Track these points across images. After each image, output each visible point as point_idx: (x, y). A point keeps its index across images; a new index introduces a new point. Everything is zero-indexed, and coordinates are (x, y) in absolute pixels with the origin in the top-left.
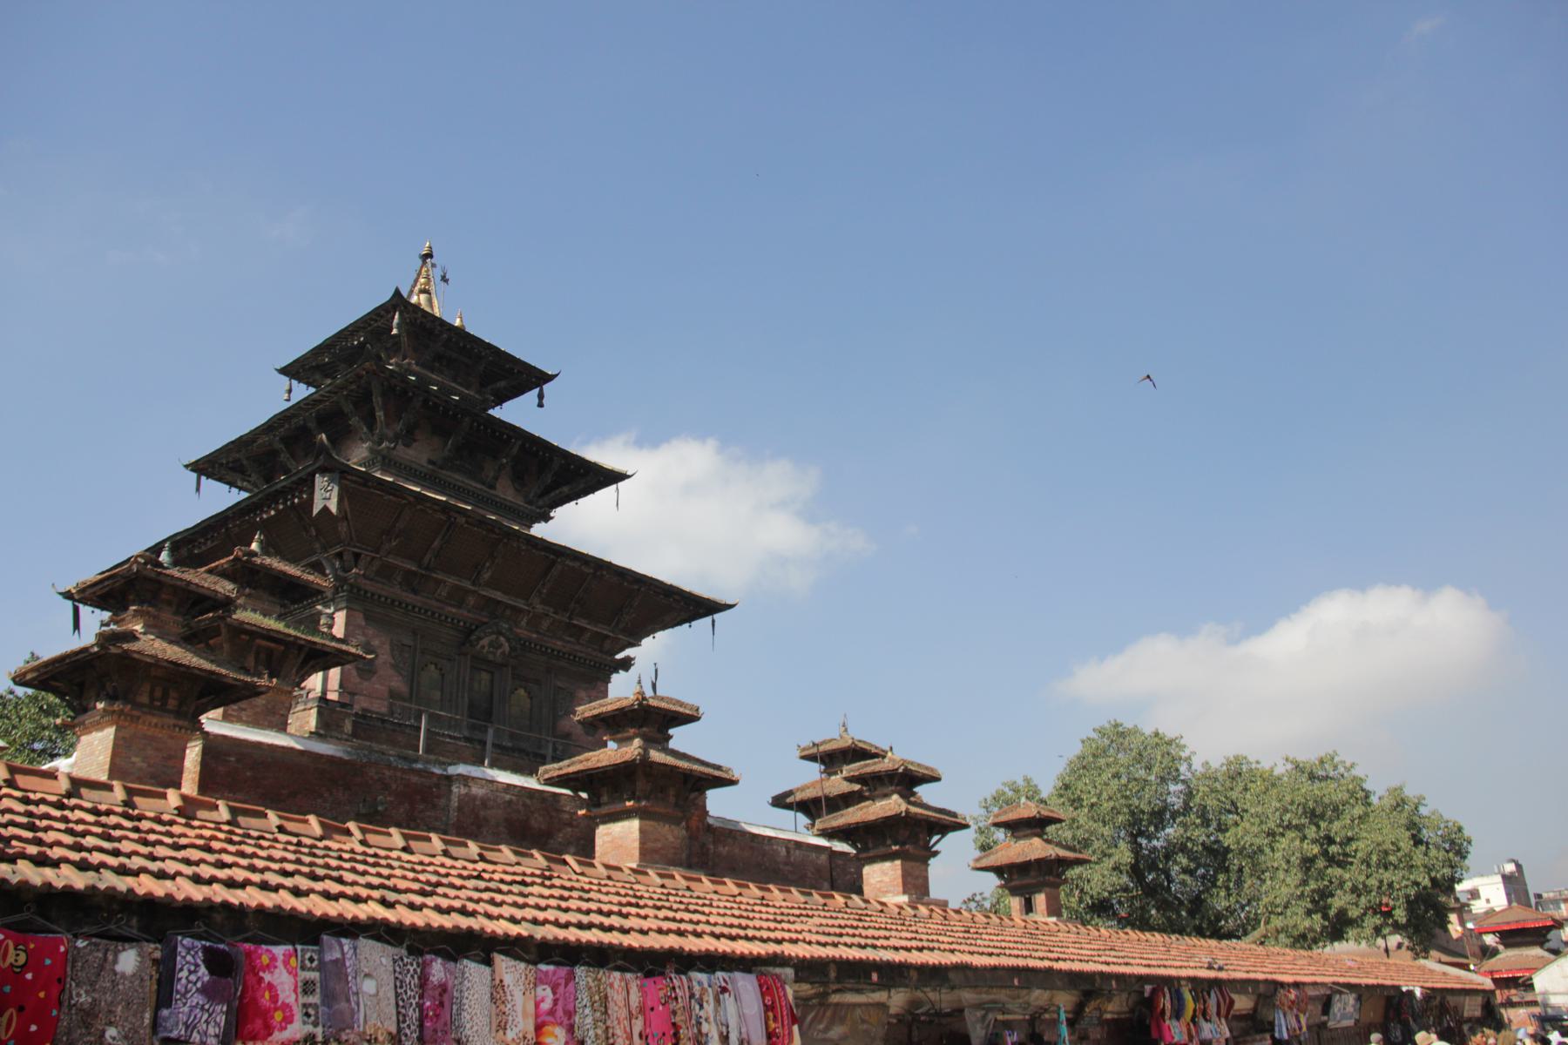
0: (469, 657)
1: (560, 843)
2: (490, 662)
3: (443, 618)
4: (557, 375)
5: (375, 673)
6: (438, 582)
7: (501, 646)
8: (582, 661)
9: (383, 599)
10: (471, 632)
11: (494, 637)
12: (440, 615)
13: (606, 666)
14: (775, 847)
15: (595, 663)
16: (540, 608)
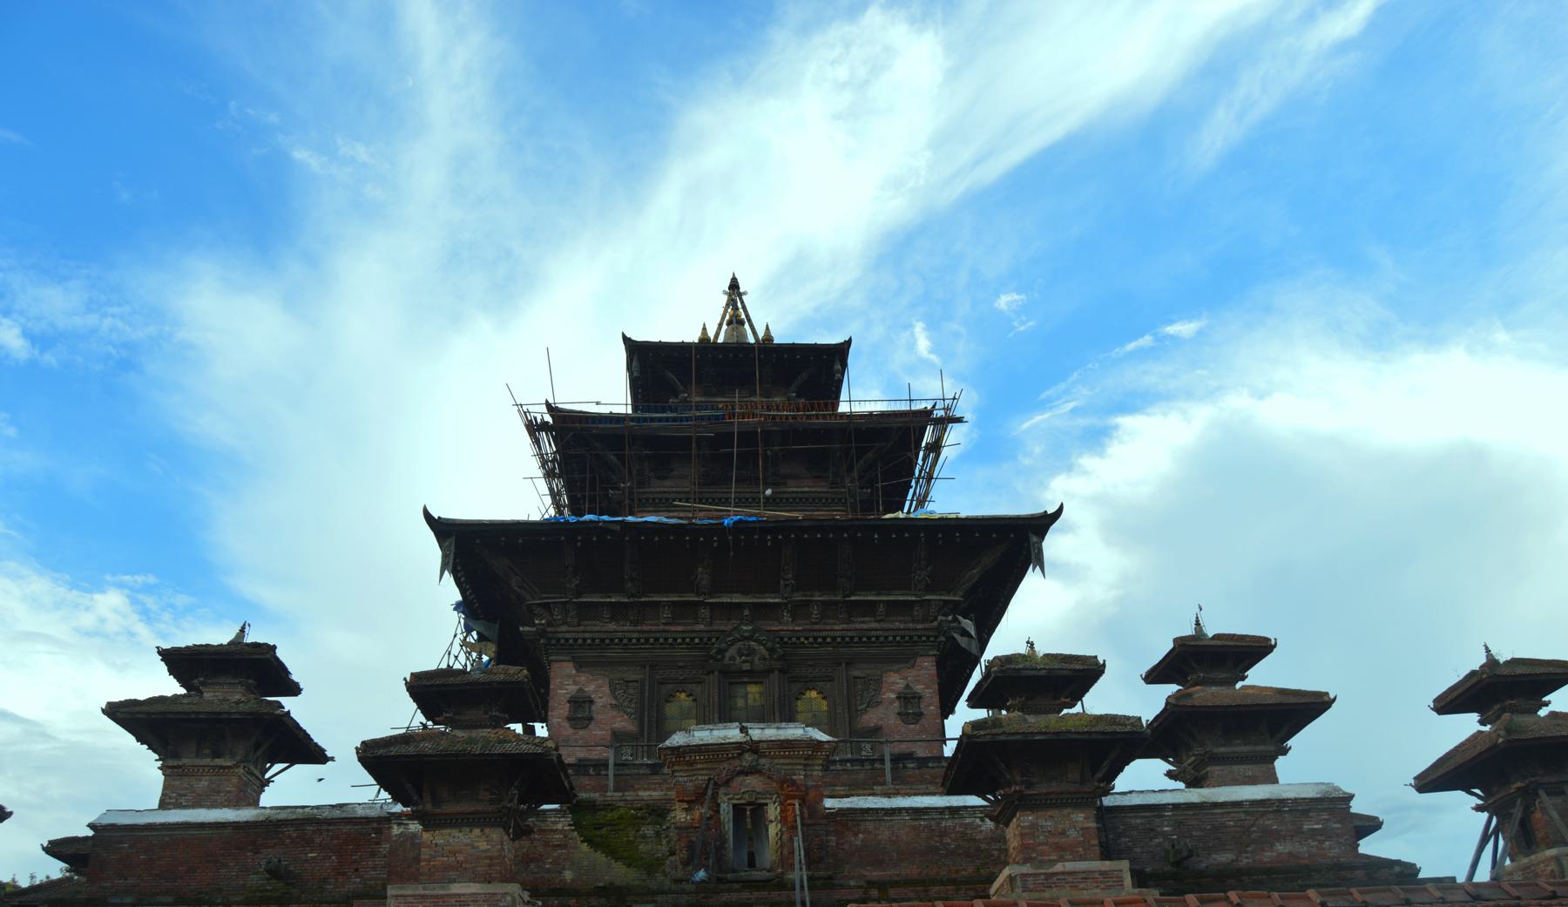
0: (716, 673)
1: (548, 871)
2: (747, 671)
3: (670, 641)
4: (848, 343)
5: (591, 719)
6: (658, 604)
7: (751, 652)
8: (882, 639)
9: (589, 641)
10: (713, 644)
11: (741, 643)
12: (666, 639)
13: (920, 637)
14: (968, 821)
15: (903, 637)
16: (798, 597)
